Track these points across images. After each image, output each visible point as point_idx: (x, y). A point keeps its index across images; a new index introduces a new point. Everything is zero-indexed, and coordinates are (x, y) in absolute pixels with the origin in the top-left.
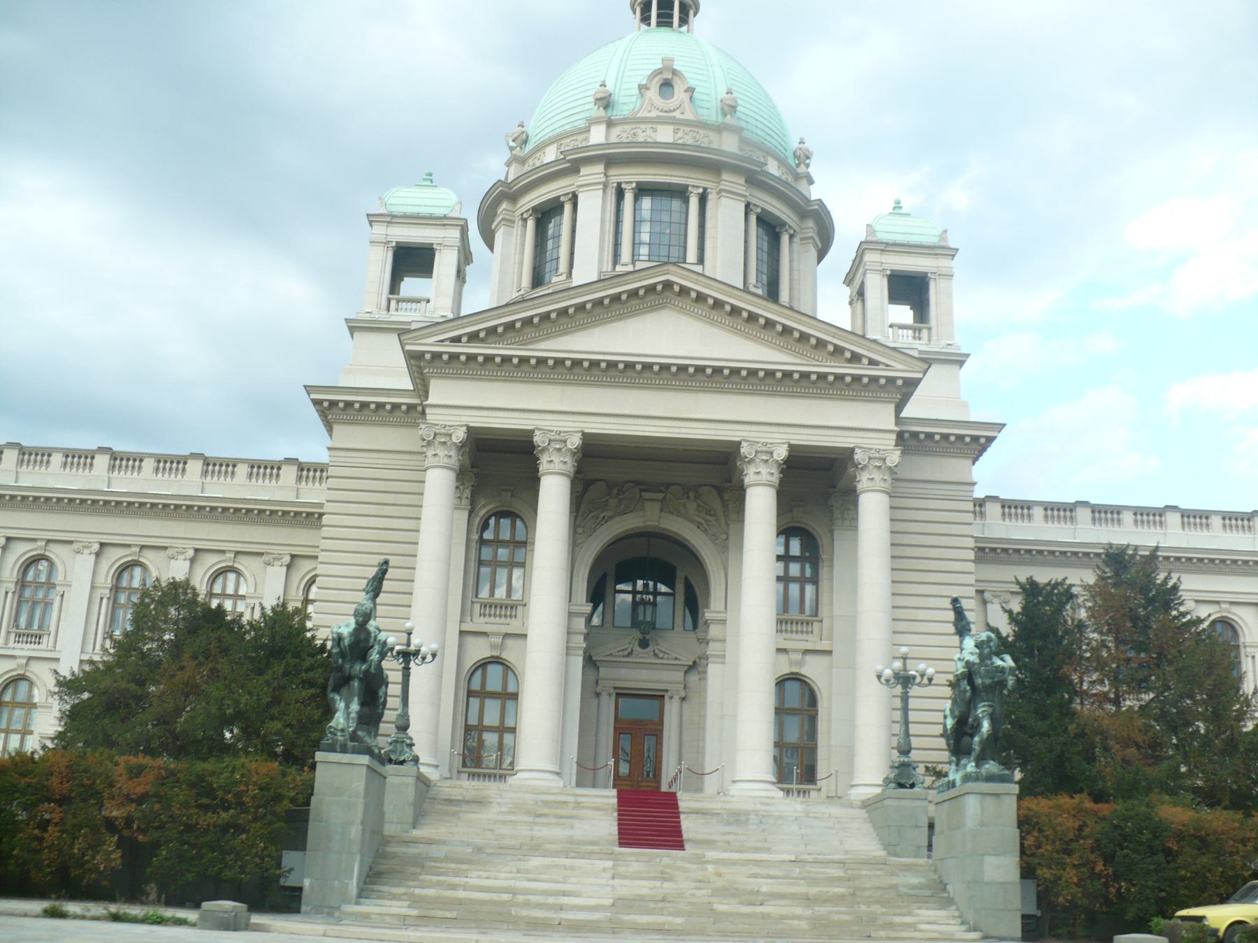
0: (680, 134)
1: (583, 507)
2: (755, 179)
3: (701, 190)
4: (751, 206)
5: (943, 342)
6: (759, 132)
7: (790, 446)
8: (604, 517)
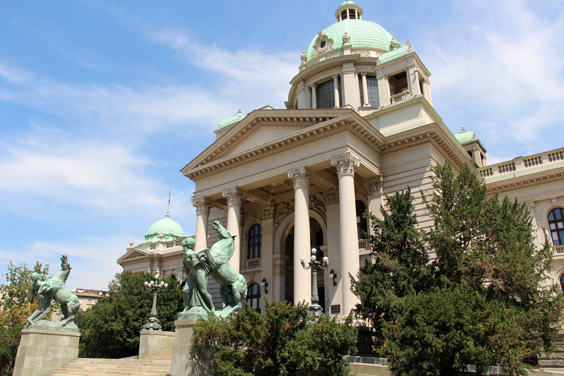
1: (277, 215)
3: (337, 76)
4: (362, 74)
8: (283, 217)
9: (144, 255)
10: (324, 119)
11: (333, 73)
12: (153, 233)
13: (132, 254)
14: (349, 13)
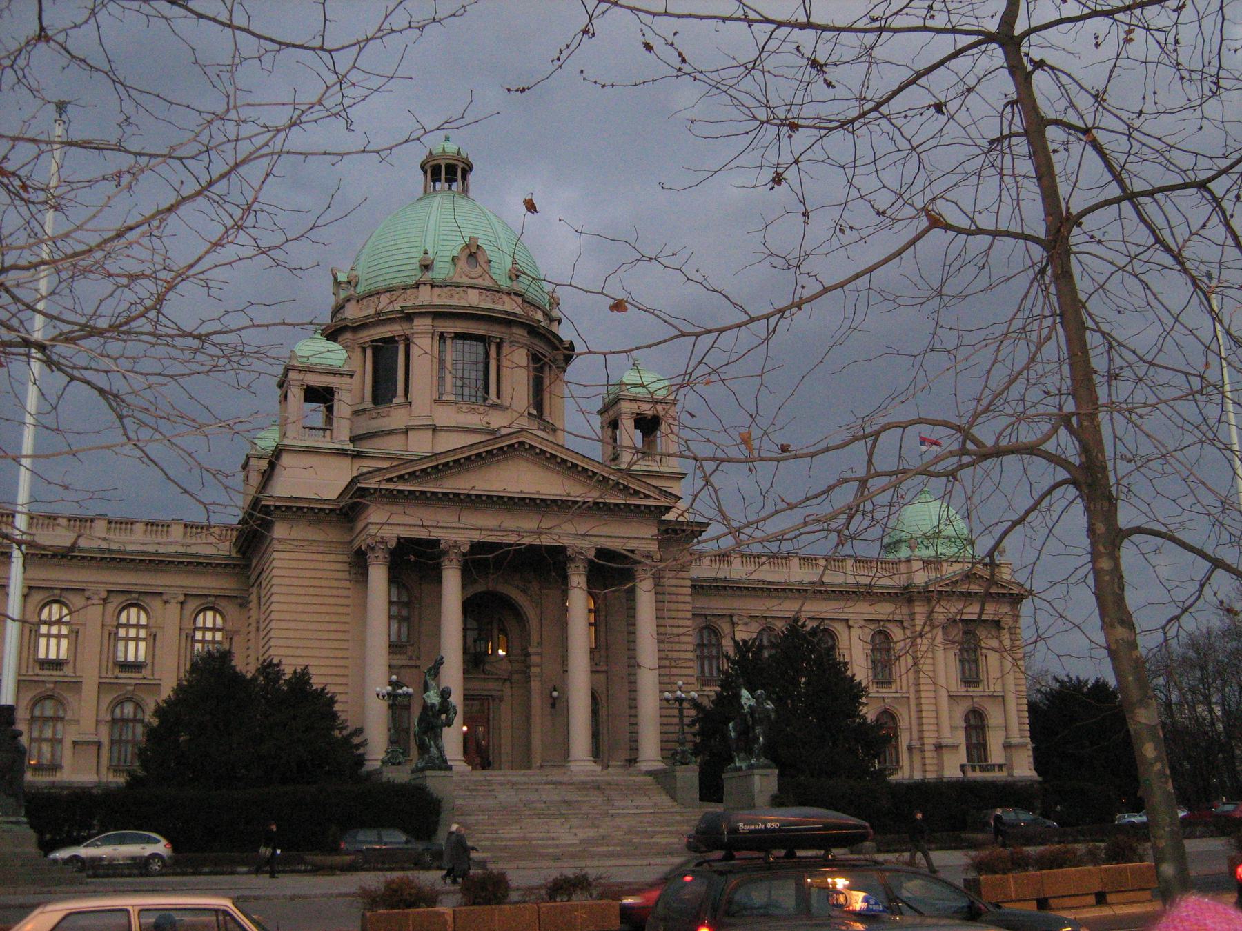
0: (484, 297)
2: (533, 330)
7: (597, 549)
11: (495, 331)
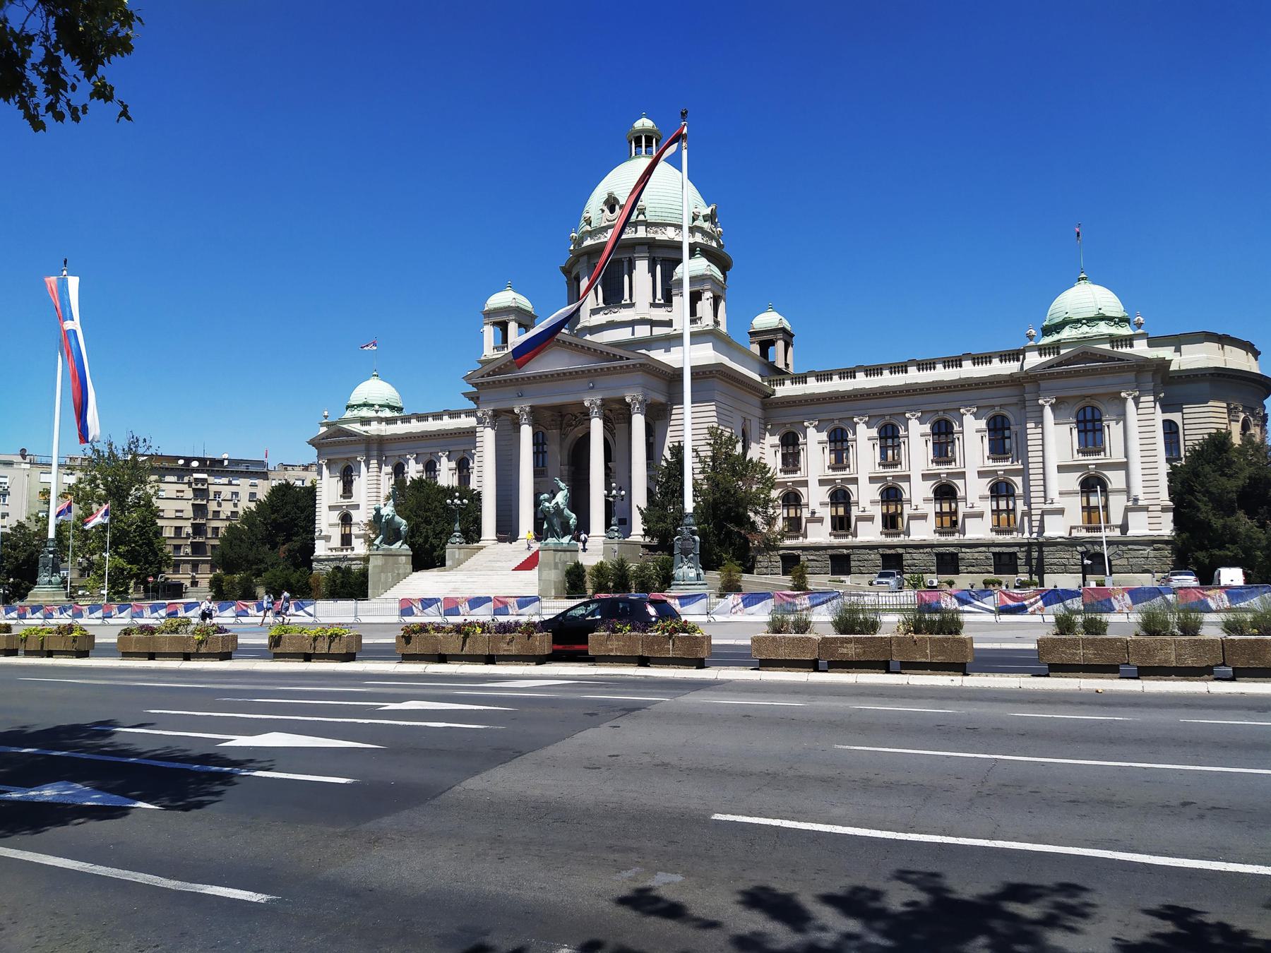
5: (704, 325)
6: (663, 214)
9: (356, 436)
10: (621, 358)
12: (361, 402)
13: (335, 432)
14: (646, 142)
